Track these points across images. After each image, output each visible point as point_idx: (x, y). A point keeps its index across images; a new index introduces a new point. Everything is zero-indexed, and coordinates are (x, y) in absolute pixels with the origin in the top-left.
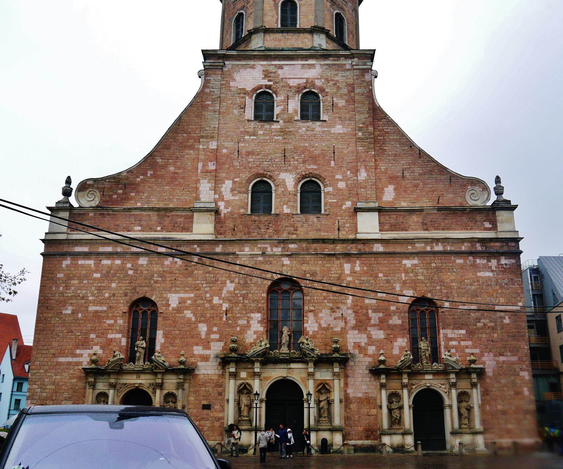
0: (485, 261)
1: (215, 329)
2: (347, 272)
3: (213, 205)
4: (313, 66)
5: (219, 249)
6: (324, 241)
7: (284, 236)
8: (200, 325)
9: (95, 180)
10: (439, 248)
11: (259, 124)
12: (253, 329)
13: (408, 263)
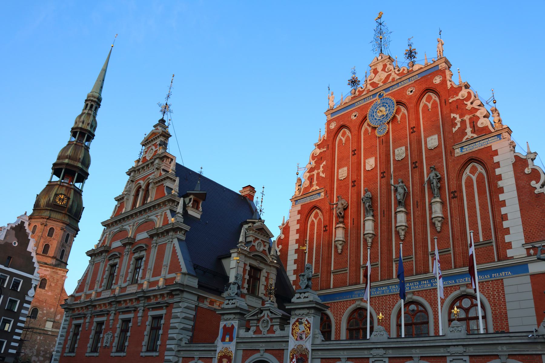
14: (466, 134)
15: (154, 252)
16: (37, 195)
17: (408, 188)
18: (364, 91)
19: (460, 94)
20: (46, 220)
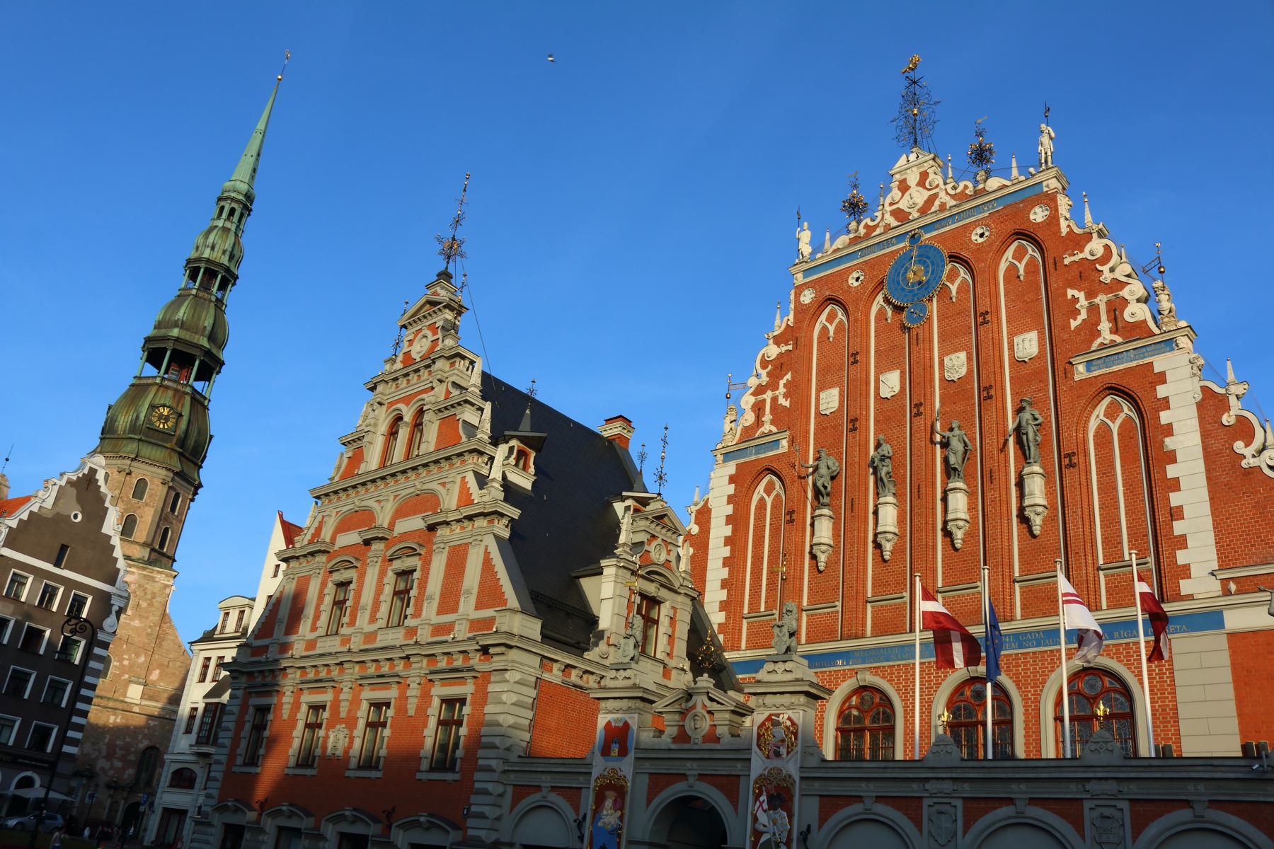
14: (1099, 333)
15: (439, 564)
17: (973, 440)
18: (877, 226)
19: (1087, 249)
20: (128, 462)
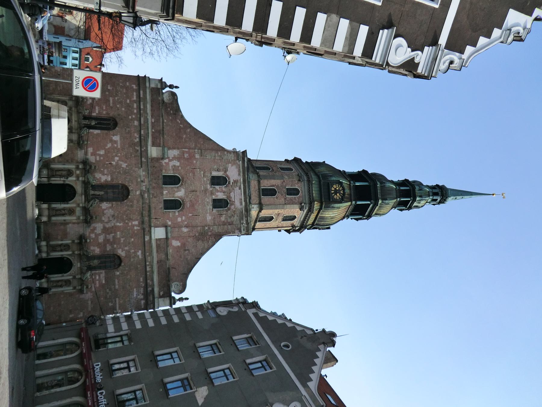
0: (142, 292)
1: (102, 158)
2: (134, 223)
3: (166, 157)
4: (241, 204)
5: (143, 159)
6: (149, 211)
7: (151, 192)
8: (104, 151)
9: (177, 100)
10: (148, 269)
11: (210, 178)
12: (102, 177)
13: (139, 253)
16: (324, 162)
